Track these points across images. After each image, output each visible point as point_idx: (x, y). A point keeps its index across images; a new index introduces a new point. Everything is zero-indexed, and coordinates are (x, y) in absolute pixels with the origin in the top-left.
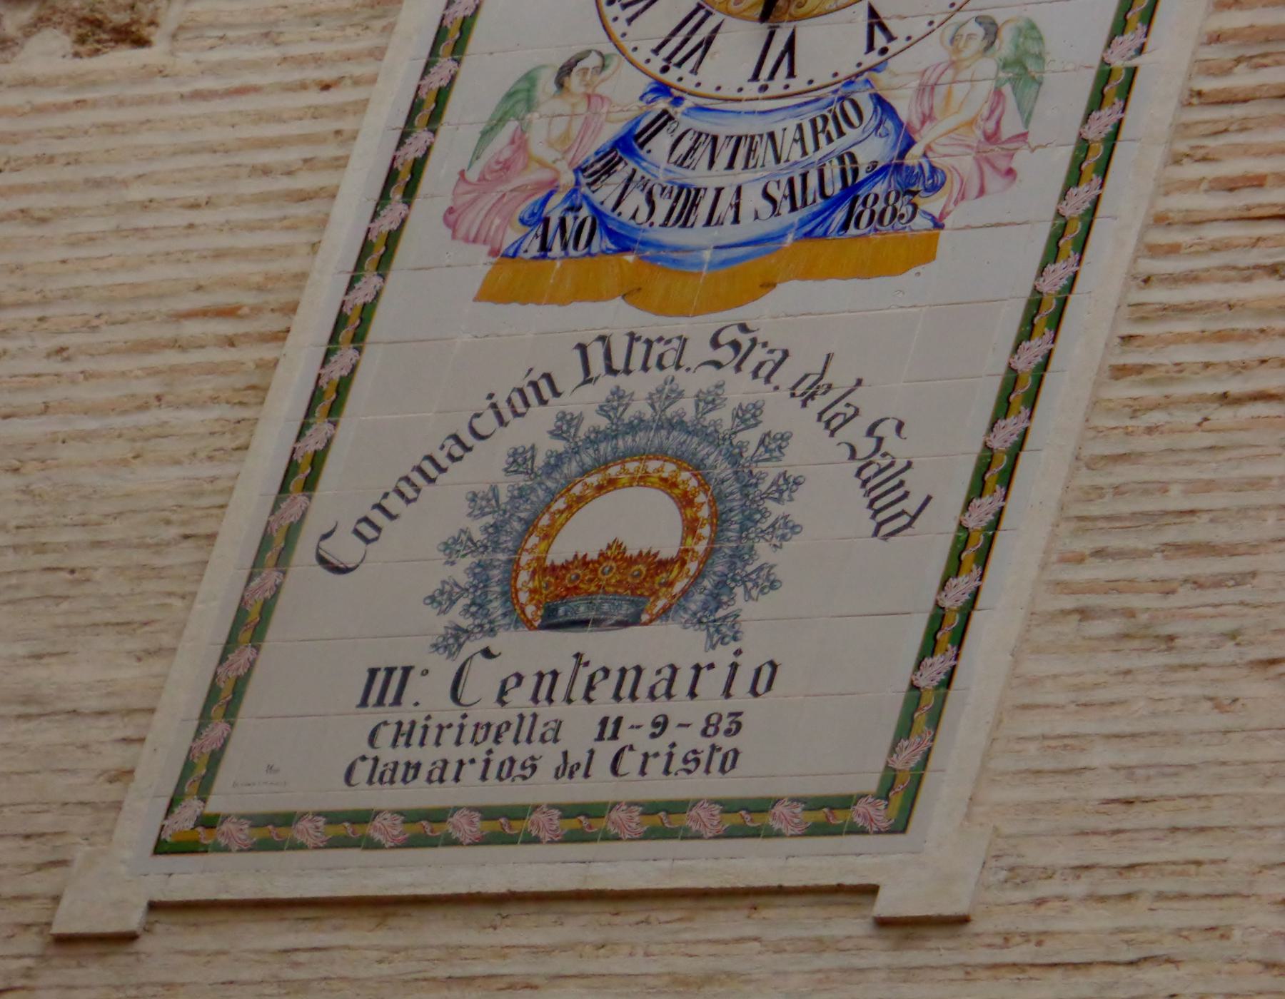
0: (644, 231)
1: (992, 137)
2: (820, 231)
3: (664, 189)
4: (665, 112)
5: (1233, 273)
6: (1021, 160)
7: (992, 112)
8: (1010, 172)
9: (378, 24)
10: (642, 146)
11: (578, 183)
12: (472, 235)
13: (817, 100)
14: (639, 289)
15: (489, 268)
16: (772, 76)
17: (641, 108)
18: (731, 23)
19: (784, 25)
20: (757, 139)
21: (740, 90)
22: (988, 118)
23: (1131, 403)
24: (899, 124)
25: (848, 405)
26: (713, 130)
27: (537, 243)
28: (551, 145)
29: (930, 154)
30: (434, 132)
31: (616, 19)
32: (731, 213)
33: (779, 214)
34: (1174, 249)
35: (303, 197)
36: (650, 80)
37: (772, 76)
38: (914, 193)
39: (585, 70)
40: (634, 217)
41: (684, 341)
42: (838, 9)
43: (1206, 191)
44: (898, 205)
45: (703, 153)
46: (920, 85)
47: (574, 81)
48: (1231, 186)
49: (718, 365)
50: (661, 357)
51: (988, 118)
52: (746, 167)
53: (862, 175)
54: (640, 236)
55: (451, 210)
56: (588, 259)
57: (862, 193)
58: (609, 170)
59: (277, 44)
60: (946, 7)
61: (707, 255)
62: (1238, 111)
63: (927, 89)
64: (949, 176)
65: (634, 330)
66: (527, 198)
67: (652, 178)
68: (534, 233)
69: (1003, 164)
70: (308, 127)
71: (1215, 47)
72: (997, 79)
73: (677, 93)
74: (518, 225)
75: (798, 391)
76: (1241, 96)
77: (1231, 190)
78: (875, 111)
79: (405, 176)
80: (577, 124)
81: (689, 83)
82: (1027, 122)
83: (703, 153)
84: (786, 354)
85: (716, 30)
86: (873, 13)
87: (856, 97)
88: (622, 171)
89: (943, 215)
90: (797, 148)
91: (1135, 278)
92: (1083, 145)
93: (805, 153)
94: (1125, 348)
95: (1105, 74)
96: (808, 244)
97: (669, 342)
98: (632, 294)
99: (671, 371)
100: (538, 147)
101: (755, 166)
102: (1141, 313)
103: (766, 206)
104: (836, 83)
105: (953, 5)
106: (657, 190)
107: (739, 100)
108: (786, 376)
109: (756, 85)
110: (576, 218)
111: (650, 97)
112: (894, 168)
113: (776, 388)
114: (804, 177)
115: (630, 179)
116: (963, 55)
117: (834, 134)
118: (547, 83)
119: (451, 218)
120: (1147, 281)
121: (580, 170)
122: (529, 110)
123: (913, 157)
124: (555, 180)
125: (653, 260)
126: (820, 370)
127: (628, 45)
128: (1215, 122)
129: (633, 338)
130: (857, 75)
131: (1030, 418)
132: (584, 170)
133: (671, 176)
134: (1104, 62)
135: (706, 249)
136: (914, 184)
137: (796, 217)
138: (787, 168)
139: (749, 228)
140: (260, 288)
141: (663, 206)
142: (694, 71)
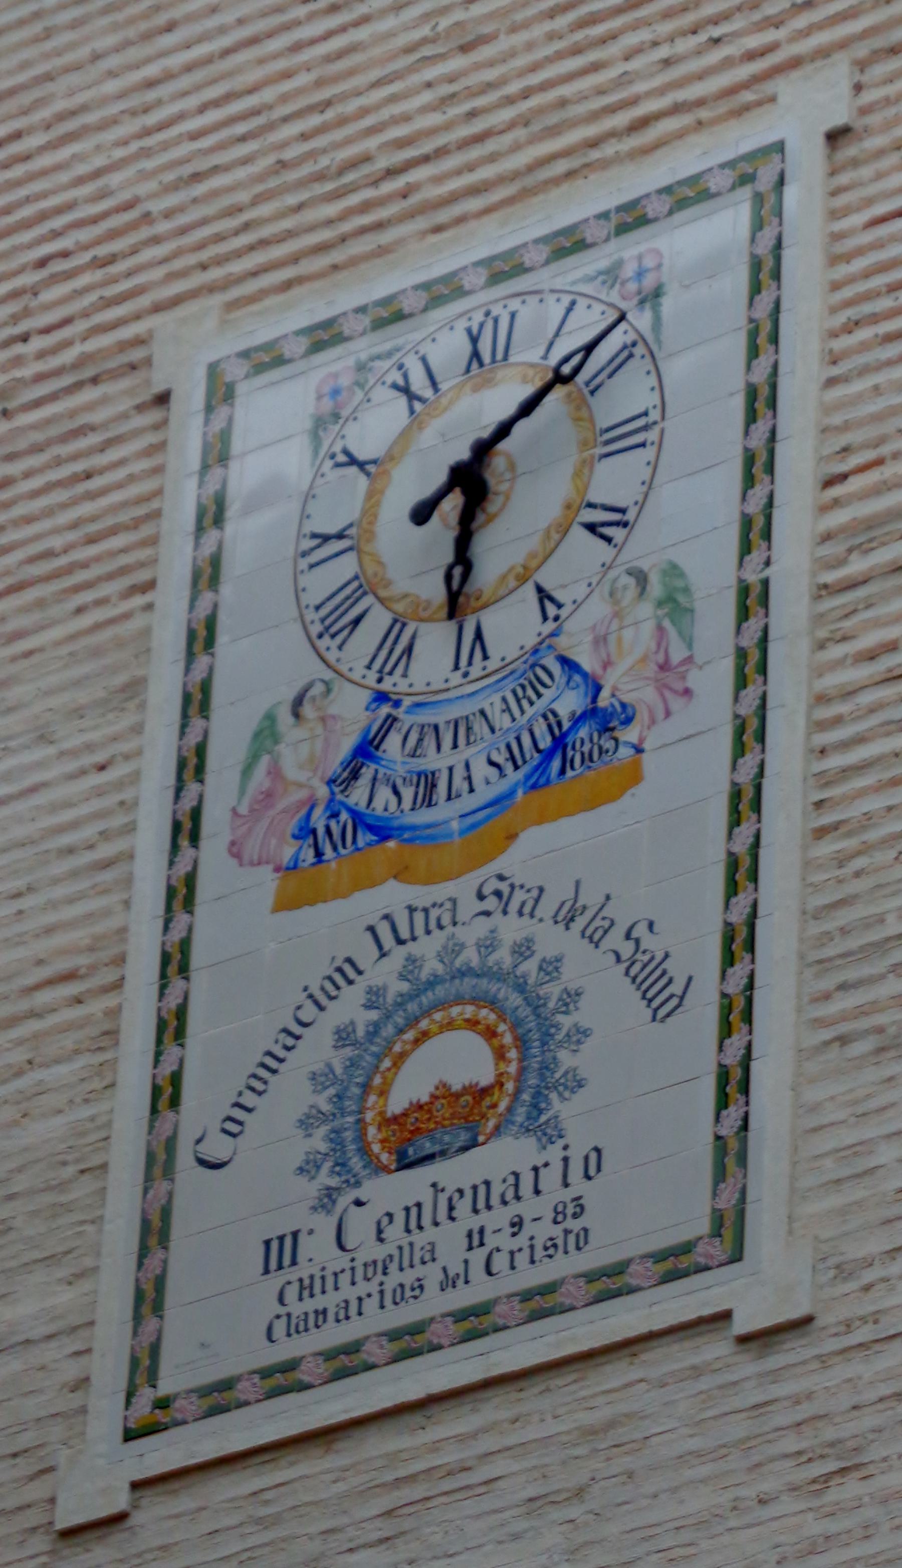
0: (397, 818)
1: (664, 667)
2: (542, 780)
3: (405, 779)
4: (389, 716)
5: (892, 727)
6: (694, 679)
7: (659, 645)
8: (687, 692)
9: (131, 705)
10: (377, 748)
11: (333, 793)
12: (256, 858)
13: (512, 673)
14: (407, 868)
15: (277, 882)
16: (470, 664)
17: (368, 717)
18: (424, 627)
19: (469, 617)
20: (471, 717)
21: (447, 681)
22: (657, 652)
23: (835, 856)
24: (585, 675)
25: (604, 918)
26: (433, 720)
27: (311, 852)
28: (301, 767)
29: (617, 693)
30: (201, 781)
31: (328, 649)
32: (465, 786)
33: (505, 775)
34: (838, 721)
35: (106, 864)
36: (370, 692)
37: (470, 664)
38: (613, 729)
39: (314, 699)
40: (386, 809)
41: (454, 901)
42: (511, 592)
43: (853, 664)
44: (602, 742)
45: (430, 742)
46: (595, 638)
47: (308, 710)
48: (871, 656)
49: (487, 914)
50: (439, 920)
51: (657, 652)
52: (468, 743)
53: (566, 725)
54: (396, 823)
55: (233, 843)
56: (357, 854)
57: (569, 740)
58: (355, 775)
59: (51, 742)
60: (600, 569)
61: (455, 825)
62: (861, 592)
63: (600, 641)
64: (637, 707)
65: (411, 902)
66: (292, 817)
67: (392, 772)
68: (305, 846)
69: (680, 686)
70: (96, 805)
71: (828, 544)
72: (657, 617)
73: (394, 697)
74: (292, 841)
75: (560, 918)
76: (860, 579)
77: (872, 658)
78: (563, 668)
79: (187, 825)
80: (319, 744)
81: (403, 686)
82: (690, 646)
83: (430, 742)
84: (541, 890)
85: (413, 637)
86: (540, 590)
87: (544, 662)
88: (367, 773)
89: (642, 740)
90: (506, 717)
91: (812, 751)
92: (742, 654)
93: (514, 720)
94: (820, 811)
95: (744, 591)
96: (536, 794)
97: (441, 905)
98: (402, 874)
99: (450, 929)
100: (291, 772)
101: (475, 741)
102: (825, 780)
103: (494, 771)
104: (522, 656)
105: (603, 565)
106: (399, 782)
107: (448, 690)
108: (546, 908)
109: (459, 673)
110: (338, 822)
111: (374, 706)
112: (591, 713)
113: (541, 920)
114: (518, 739)
115: (375, 779)
116: (625, 603)
117: (534, 697)
118: (285, 717)
119: (235, 850)
120: (822, 752)
121: (331, 782)
122: (276, 742)
123: (604, 700)
124: (312, 796)
125: (410, 840)
126: (572, 895)
127: (344, 668)
128: (844, 606)
129: (411, 910)
130: (541, 643)
131: (756, 890)
132: (334, 781)
133: (407, 767)
134: (741, 581)
135: (452, 819)
136: (609, 722)
137: (520, 775)
138: (502, 736)
139: (484, 794)
140: (91, 949)
141: (407, 793)
142: (405, 675)
